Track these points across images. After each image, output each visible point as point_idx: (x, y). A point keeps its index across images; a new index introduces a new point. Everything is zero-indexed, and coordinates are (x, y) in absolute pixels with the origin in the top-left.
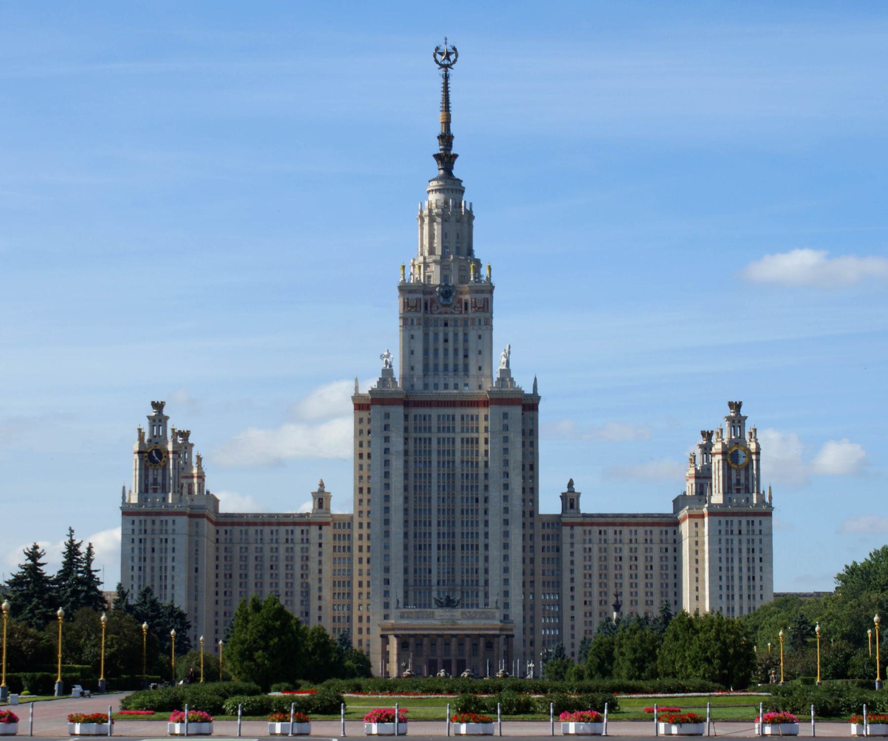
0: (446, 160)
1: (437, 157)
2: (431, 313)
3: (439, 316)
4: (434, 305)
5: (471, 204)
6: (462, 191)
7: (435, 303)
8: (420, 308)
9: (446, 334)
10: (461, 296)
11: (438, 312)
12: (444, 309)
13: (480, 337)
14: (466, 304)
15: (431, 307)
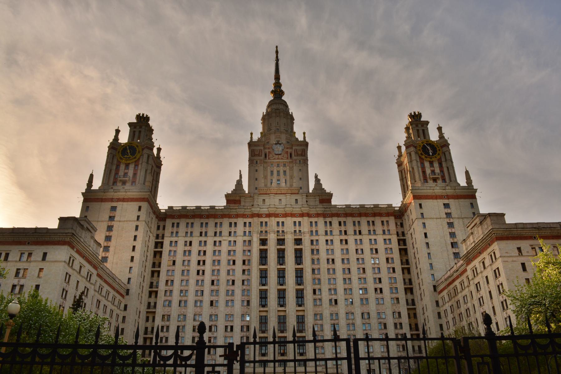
0: (278, 92)
1: (272, 92)
2: (269, 159)
3: (273, 161)
4: (271, 156)
5: (292, 113)
6: (287, 106)
7: (271, 153)
8: (262, 154)
9: (278, 172)
10: (287, 150)
11: (273, 158)
12: (277, 156)
13: (300, 170)
14: (291, 154)
15: (269, 156)
